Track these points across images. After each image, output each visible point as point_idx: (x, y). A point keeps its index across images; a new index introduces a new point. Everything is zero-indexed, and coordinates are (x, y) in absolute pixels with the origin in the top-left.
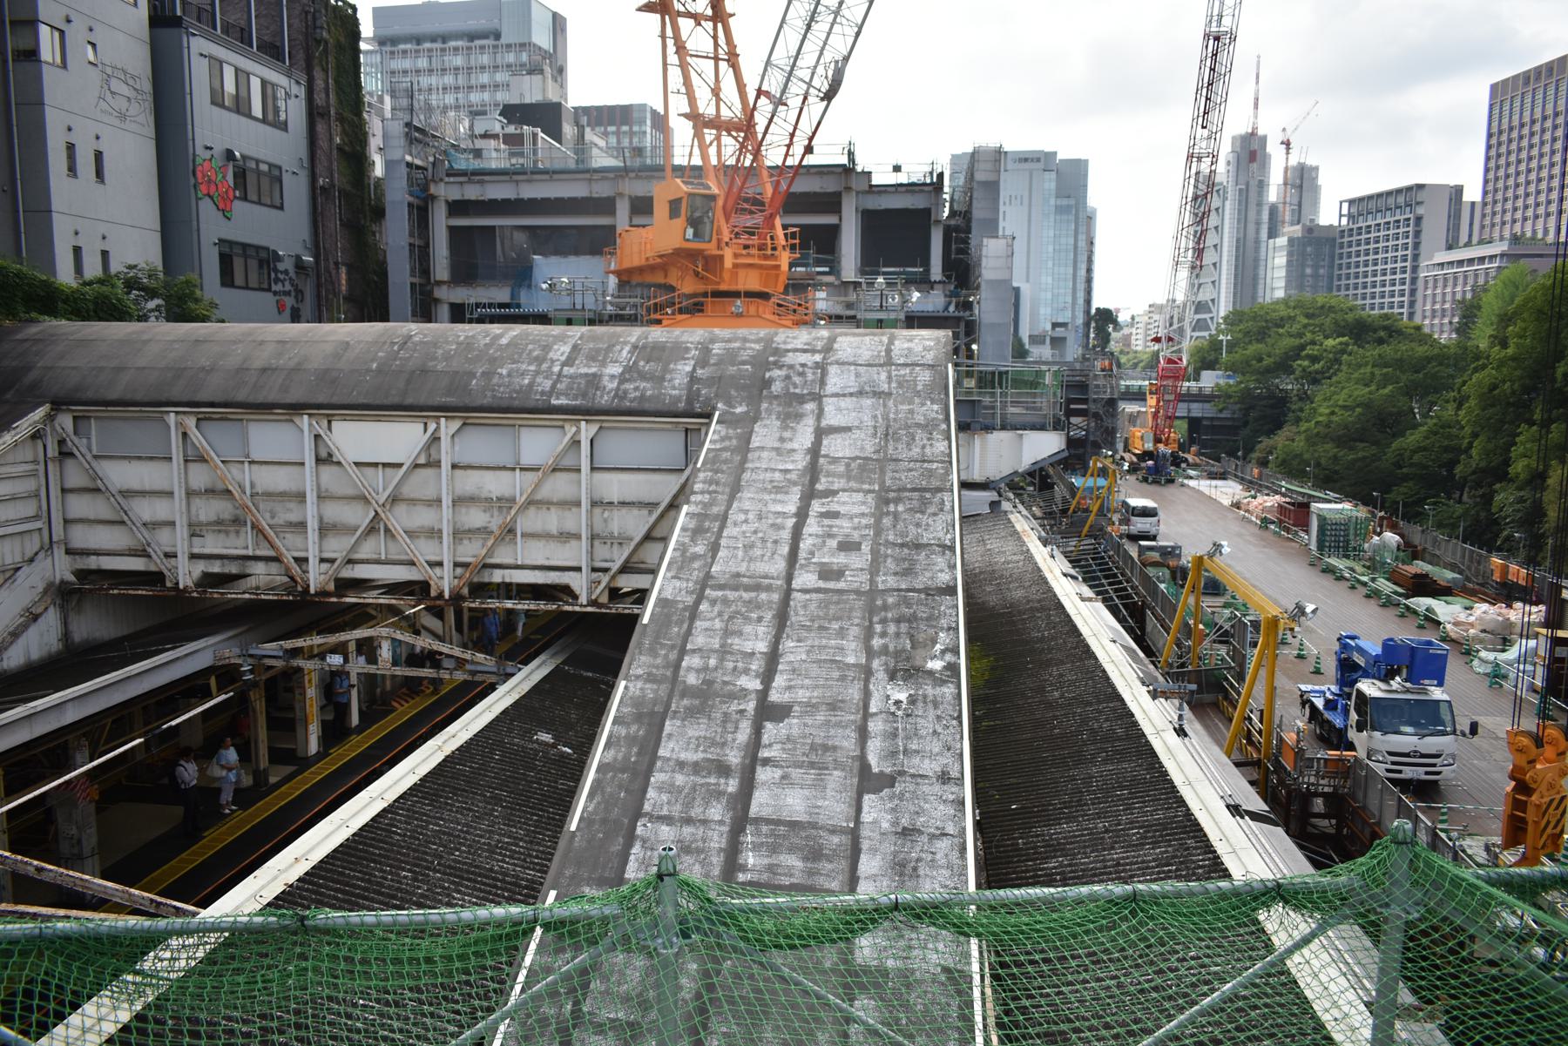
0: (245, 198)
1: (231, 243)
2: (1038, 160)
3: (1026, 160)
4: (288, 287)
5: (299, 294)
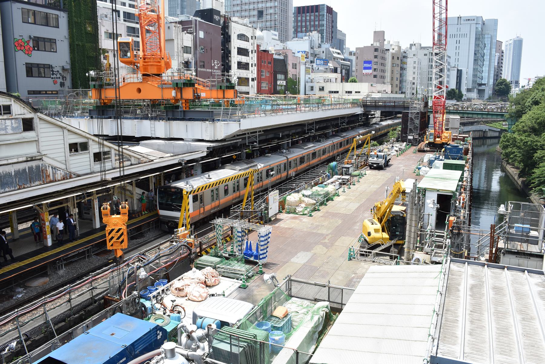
0: (38, 50)
1: (31, 64)
2: (474, 20)
3: (469, 20)
4: (58, 76)
5: (63, 77)
